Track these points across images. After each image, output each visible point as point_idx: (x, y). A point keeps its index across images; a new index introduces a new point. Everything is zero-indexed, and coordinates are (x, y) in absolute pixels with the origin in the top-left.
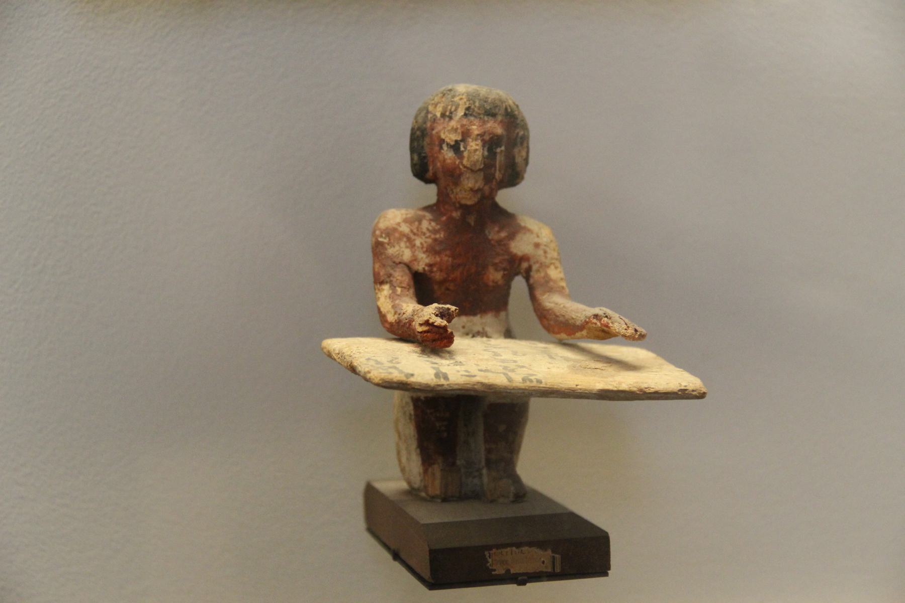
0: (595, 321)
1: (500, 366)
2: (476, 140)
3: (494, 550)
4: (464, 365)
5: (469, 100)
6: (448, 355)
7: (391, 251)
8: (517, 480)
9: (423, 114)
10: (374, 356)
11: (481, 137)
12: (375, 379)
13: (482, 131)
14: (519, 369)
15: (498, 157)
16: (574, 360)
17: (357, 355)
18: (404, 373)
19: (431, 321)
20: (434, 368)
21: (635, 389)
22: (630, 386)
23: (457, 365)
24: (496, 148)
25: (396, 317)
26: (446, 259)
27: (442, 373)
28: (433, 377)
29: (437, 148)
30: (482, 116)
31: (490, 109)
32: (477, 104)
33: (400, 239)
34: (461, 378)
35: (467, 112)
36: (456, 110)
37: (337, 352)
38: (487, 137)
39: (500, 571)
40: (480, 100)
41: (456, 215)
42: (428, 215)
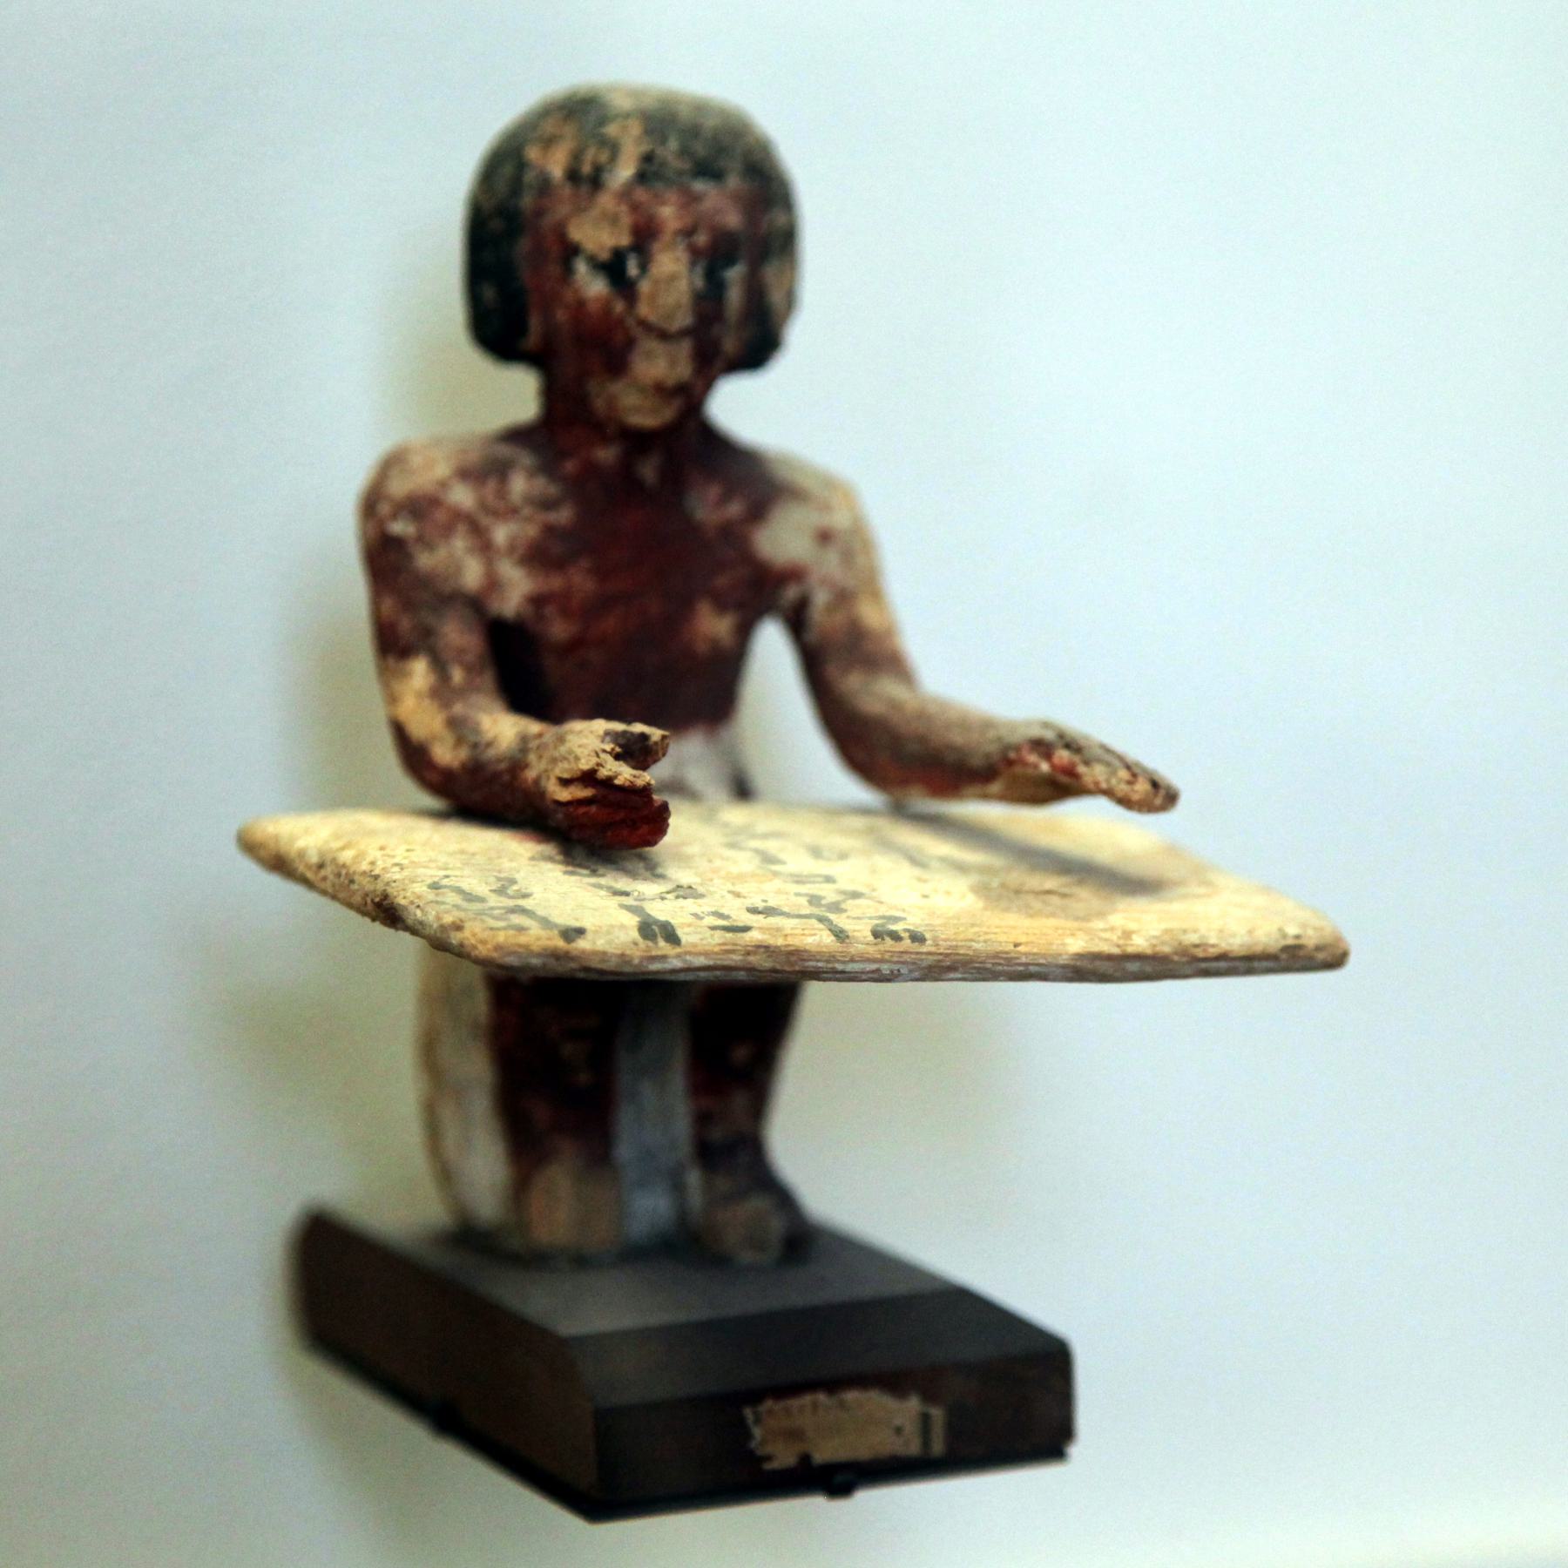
0: (1032, 758)
1: (798, 894)
3: (769, 1404)
4: (702, 896)
6: (641, 865)
7: (425, 561)
8: (784, 1198)
9: (508, 170)
10: (447, 877)
12: (480, 947)
14: (850, 902)
16: (984, 870)
17: (395, 874)
18: (556, 926)
19: (603, 773)
20: (629, 908)
21: (1166, 949)
22: (1154, 942)
23: (685, 898)
25: (463, 754)
26: (580, 580)
27: (656, 922)
28: (635, 935)
29: (554, 269)
33: (448, 530)
34: (712, 936)
37: (314, 859)
38: (702, 239)
39: (783, 1457)
41: (606, 455)
42: (526, 459)
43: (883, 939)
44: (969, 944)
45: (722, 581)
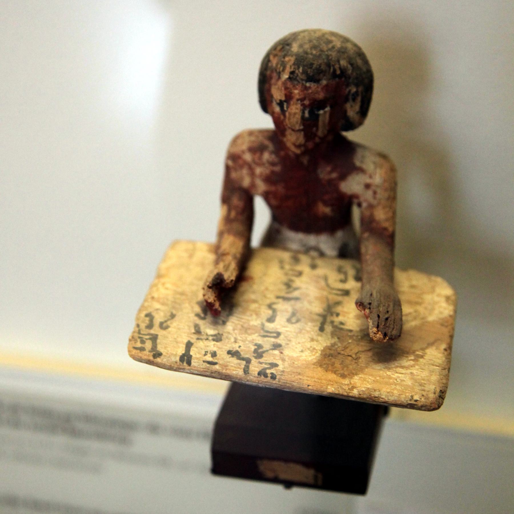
2: (296, 104)
5: (294, 64)
11: (301, 101)
13: (302, 96)
15: (321, 119)
24: (319, 110)
30: (304, 82)
31: (313, 75)
32: (301, 70)
33: (241, 167)
35: (291, 76)
36: (283, 70)
38: (307, 102)
39: (270, 475)
40: (304, 66)
42: (271, 147)
43: (261, 376)
44: (291, 383)
45: (326, 197)
